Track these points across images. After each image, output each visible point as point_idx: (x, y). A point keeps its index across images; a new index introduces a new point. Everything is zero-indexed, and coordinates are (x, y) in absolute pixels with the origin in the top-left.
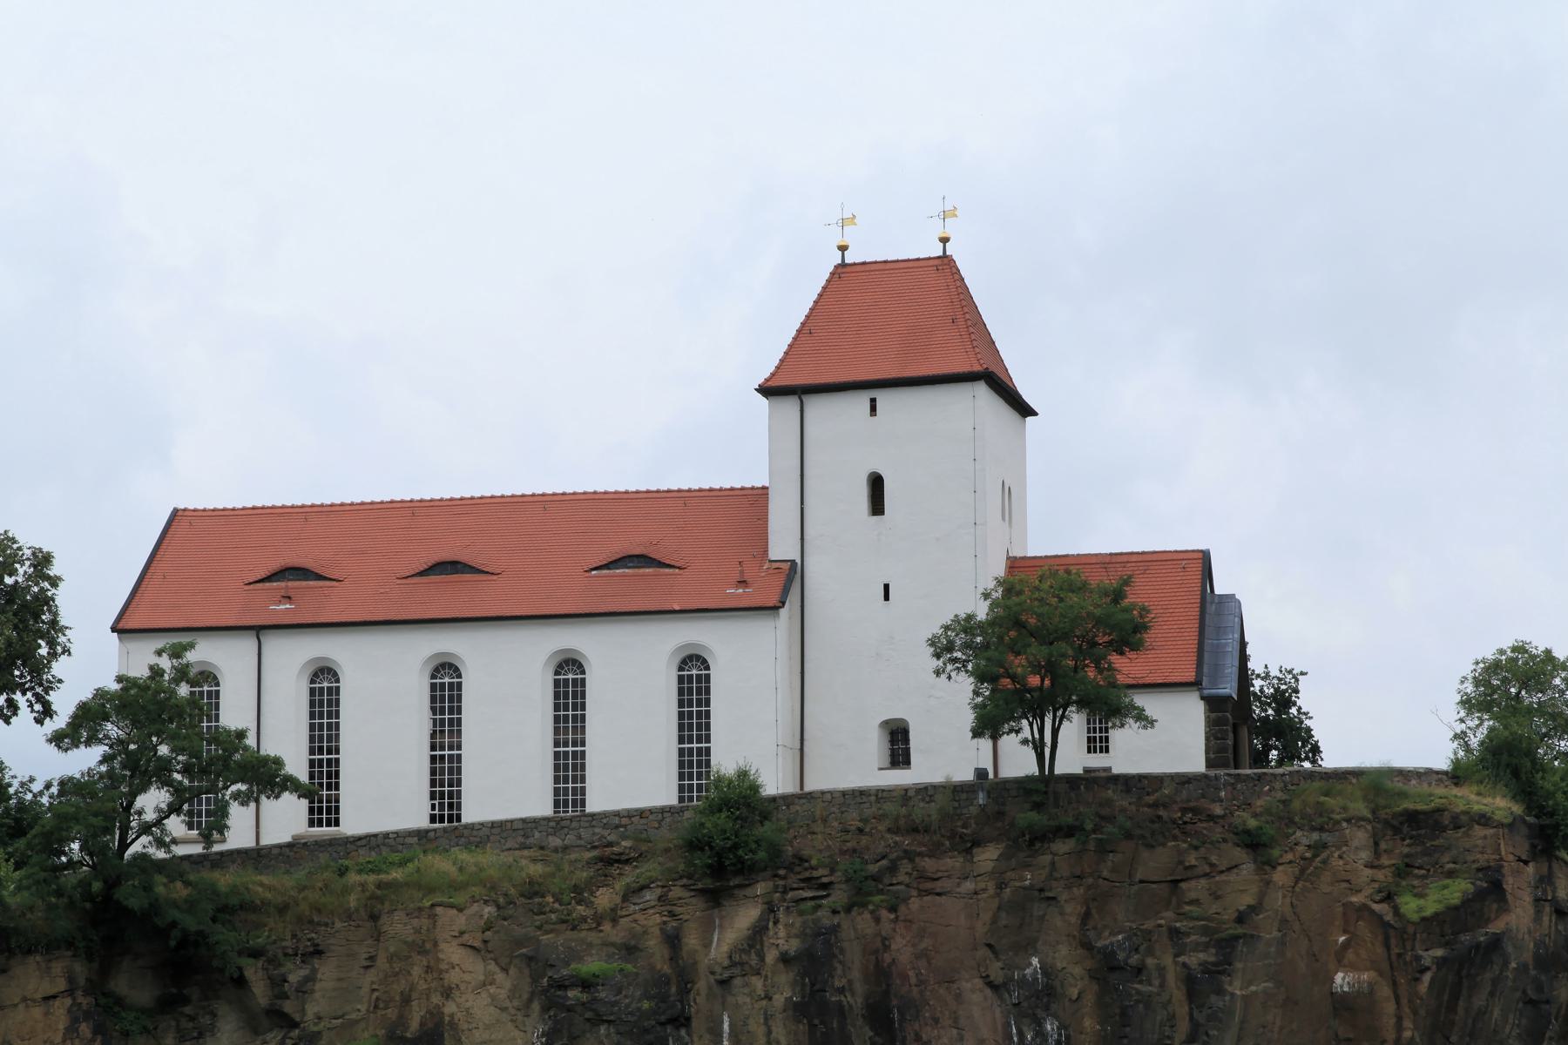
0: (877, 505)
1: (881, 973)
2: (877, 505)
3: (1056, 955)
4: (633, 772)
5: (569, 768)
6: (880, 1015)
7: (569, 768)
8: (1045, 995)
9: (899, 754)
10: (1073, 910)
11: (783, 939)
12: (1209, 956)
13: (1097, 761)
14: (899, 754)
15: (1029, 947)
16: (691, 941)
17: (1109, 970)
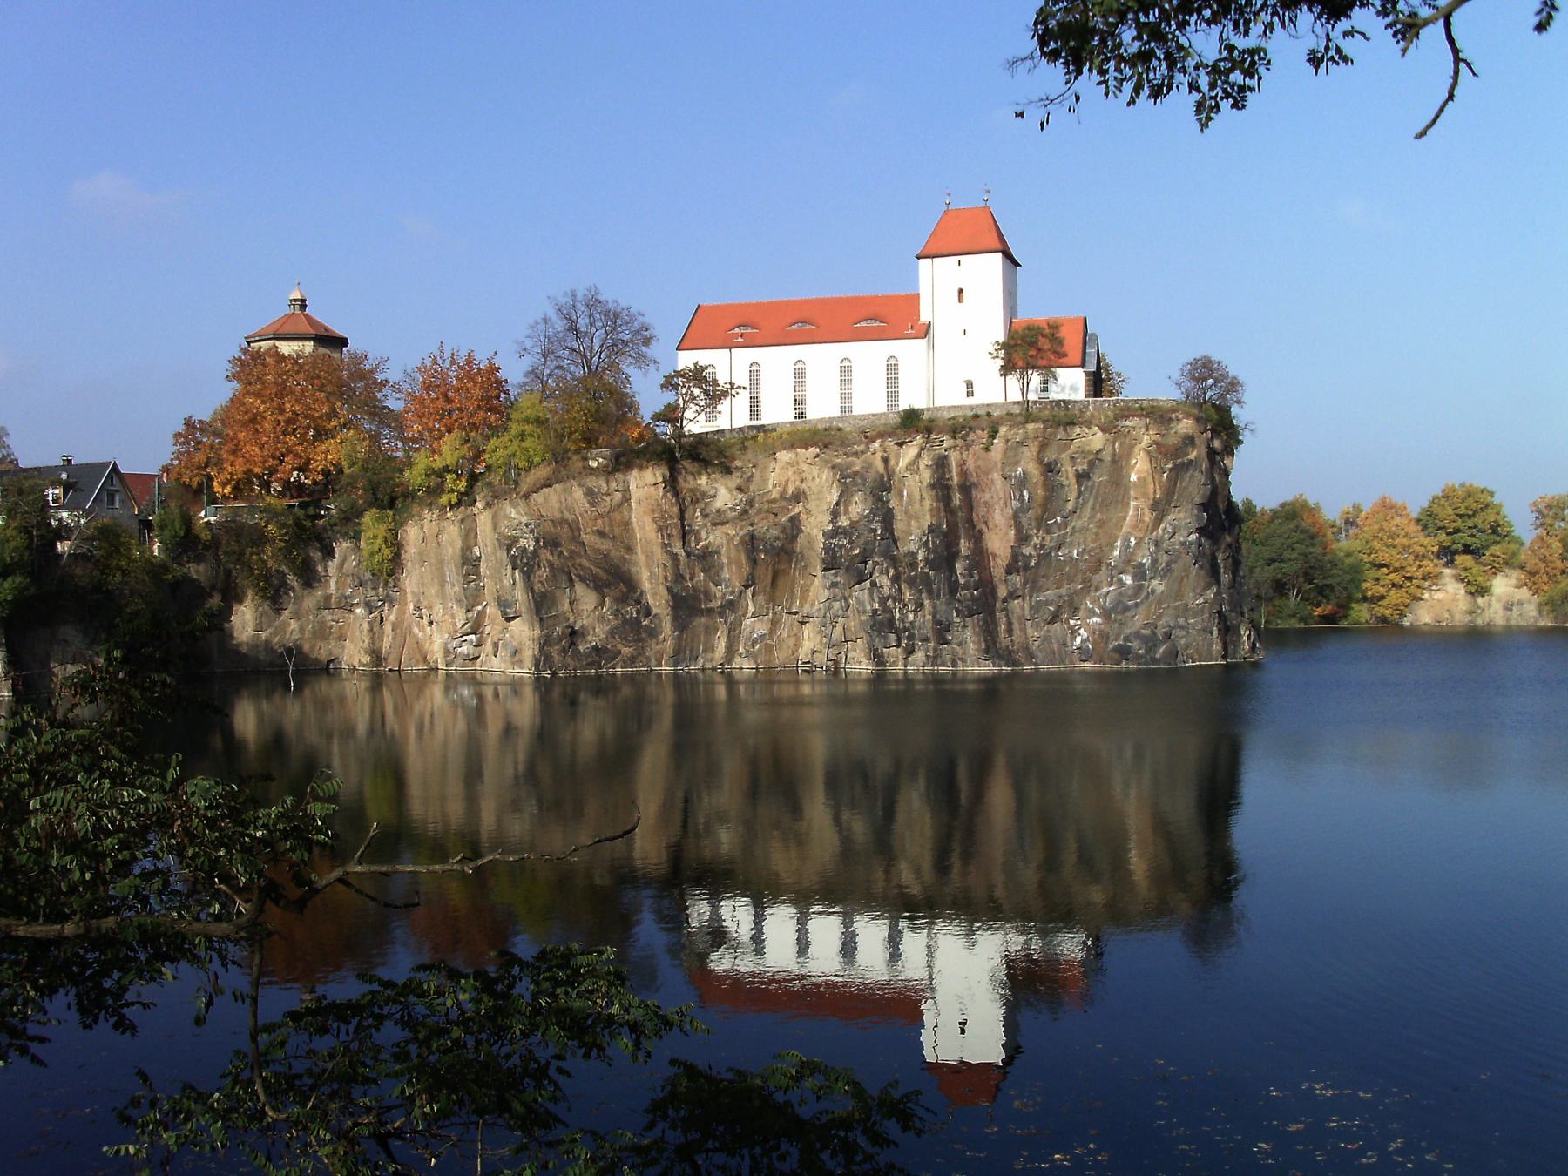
0: (960, 300)
1: (964, 473)
2: (960, 300)
3: (1028, 465)
4: (870, 402)
5: (845, 398)
6: (966, 489)
7: (845, 398)
8: (1023, 482)
9: (970, 394)
10: (1033, 448)
11: (926, 460)
12: (1085, 467)
13: (1043, 395)
14: (970, 394)
15: (1017, 463)
16: (892, 462)
17: (1050, 469)
